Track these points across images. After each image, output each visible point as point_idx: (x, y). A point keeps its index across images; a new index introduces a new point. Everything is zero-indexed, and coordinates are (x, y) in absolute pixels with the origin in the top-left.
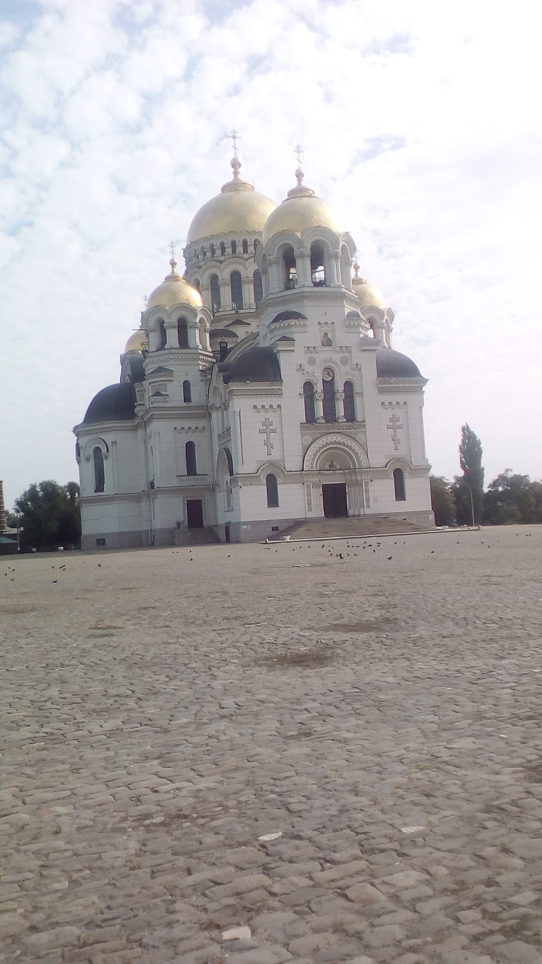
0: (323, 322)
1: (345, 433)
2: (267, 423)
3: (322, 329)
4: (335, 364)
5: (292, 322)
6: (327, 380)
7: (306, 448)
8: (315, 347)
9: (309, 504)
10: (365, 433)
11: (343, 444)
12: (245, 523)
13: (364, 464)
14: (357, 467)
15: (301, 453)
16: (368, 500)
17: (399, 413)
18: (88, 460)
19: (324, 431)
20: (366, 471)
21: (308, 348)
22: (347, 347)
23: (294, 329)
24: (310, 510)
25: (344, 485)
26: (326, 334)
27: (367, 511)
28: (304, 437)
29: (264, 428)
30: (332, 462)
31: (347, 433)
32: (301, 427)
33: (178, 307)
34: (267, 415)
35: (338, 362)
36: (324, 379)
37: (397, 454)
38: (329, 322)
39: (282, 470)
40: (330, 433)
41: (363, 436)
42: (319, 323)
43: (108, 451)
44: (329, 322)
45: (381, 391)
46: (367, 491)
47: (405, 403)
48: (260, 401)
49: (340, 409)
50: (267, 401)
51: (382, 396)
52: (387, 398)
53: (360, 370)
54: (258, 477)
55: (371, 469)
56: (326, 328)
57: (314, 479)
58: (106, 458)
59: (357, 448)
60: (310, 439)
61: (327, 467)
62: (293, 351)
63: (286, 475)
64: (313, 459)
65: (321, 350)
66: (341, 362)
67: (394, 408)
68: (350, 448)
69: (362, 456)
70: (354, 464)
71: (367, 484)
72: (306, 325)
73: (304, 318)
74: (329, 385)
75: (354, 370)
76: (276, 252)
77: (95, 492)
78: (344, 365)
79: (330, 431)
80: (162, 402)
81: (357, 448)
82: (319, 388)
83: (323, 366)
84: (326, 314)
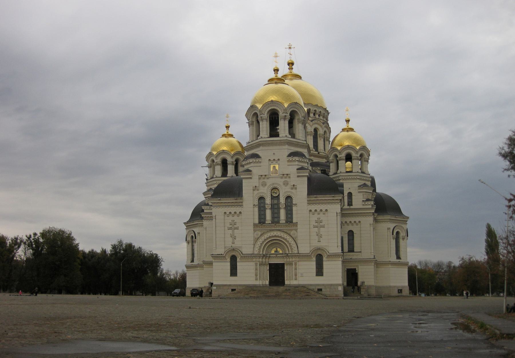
0: (272, 159)
1: (282, 230)
2: (233, 223)
3: (272, 163)
4: (279, 185)
5: (251, 160)
6: (275, 196)
7: (256, 240)
8: (265, 175)
9: (256, 275)
10: (296, 230)
11: (281, 237)
13: (295, 251)
14: (290, 252)
15: (252, 242)
16: (296, 275)
17: (322, 216)
18: (188, 243)
20: (295, 256)
21: (261, 176)
22: (287, 175)
23: (252, 165)
24: (256, 279)
25: (284, 264)
26: (274, 167)
27: (294, 282)
28: (256, 233)
29: (231, 226)
30: (277, 249)
31: (285, 231)
32: (254, 226)
33: (221, 153)
34: (233, 218)
36: (273, 195)
37: (319, 245)
38: (276, 159)
39: (239, 253)
40: (273, 230)
41: (295, 232)
42: (270, 160)
43: (195, 238)
44: (276, 159)
45: (310, 203)
46: (296, 269)
47: (326, 210)
48: (228, 210)
49: (283, 213)
50: (233, 210)
51: (310, 206)
52: (313, 207)
53: (296, 189)
54: (224, 257)
56: (274, 162)
57: (261, 260)
58: (195, 242)
60: (260, 233)
61: (273, 252)
62: (251, 178)
63: (242, 256)
64: (260, 247)
65: (270, 177)
66: (284, 184)
67: (319, 214)
68: (286, 239)
70: (289, 250)
71: (296, 264)
72: (260, 162)
75: (292, 189)
76: (251, 118)
77: (191, 262)
78: (286, 186)
79: (273, 229)
80: (209, 209)
81: (290, 240)
82: (268, 201)
83: (272, 187)
84: (274, 154)
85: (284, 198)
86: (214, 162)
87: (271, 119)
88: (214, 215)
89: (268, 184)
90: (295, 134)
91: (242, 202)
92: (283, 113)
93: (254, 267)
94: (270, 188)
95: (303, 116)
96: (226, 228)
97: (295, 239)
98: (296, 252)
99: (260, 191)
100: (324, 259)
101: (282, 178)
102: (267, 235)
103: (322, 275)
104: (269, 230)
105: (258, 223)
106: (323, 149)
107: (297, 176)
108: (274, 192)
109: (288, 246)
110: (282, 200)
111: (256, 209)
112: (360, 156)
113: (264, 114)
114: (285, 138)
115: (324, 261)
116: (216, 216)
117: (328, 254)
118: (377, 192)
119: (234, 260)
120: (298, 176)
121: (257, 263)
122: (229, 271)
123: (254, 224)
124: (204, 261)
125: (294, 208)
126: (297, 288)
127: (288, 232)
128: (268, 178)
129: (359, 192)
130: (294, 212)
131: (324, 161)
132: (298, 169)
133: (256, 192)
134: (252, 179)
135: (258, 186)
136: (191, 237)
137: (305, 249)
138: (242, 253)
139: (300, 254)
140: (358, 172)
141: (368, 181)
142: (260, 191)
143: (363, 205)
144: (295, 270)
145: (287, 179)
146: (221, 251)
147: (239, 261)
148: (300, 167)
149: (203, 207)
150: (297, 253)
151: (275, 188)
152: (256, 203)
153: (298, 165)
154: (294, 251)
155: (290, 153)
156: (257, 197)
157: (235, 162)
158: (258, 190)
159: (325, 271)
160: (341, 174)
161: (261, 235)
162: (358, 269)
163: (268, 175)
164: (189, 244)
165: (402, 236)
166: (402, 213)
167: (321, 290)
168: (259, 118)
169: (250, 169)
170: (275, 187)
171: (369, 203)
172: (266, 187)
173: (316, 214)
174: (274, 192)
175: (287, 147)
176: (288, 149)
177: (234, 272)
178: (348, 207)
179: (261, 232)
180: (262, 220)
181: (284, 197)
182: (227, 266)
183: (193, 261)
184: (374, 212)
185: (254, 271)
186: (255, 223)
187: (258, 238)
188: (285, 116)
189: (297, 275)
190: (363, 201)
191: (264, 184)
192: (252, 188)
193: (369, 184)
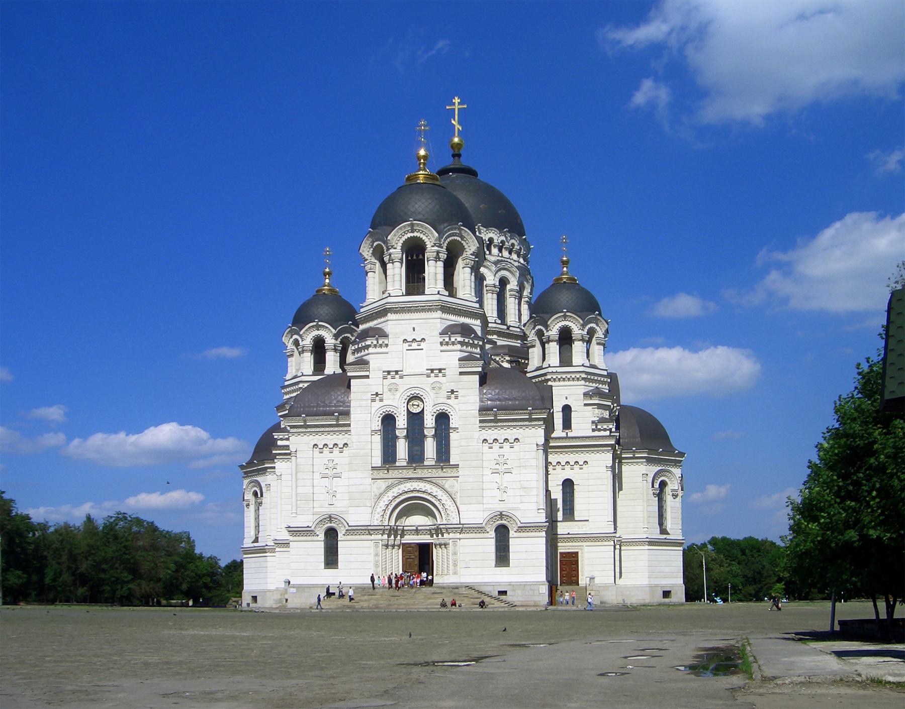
8: (397, 372)
12: (295, 586)
14: (445, 522)
16: (455, 565)
19: (400, 476)
21: (389, 372)
22: (440, 370)
23: (371, 350)
35: (428, 389)
36: (411, 410)
37: (501, 507)
42: (405, 341)
43: (262, 496)
46: (455, 554)
48: (321, 440)
49: (430, 447)
50: (330, 439)
52: (491, 434)
53: (456, 398)
54: (312, 531)
55: (461, 526)
59: (444, 498)
60: (383, 484)
62: (367, 377)
66: (433, 388)
69: (451, 507)
71: (455, 545)
73: (385, 336)
74: (415, 419)
75: (449, 398)
81: (444, 498)
82: (402, 422)
85: (433, 416)
86: (299, 346)
87: (410, 258)
88: (292, 449)
89: (401, 390)
90: (456, 288)
91: (349, 425)
92: (432, 246)
93: (372, 550)
94: (405, 397)
95: (474, 252)
96: (317, 476)
97: (453, 496)
98: (456, 521)
99: (385, 402)
100: (512, 533)
101: (428, 376)
102: (399, 489)
103: (507, 565)
104: (402, 480)
105: (380, 465)
106: (518, 321)
107: (459, 373)
108: (413, 405)
109: (441, 510)
110: (429, 421)
111: (378, 439)
112: (588, 334)
113: (395, 248)
114: (437, 297)
115: (511, 538)
116: (296, 451)
117: (519, 524)
118: (621, 404)
119: (331, 535)
120: (461, 373)
121: (379, 542)
122: (322, 558)
123: (372, 467)
124: (276, 540)
125: (453, 436)
126: (456, 590)
127: (440, 482)
128: (401, 377)
129: (586, 405)
130: (453, 443)
131: (517, 343)
132: (460, 360)
133: (377, 404)
134: (369, 378)
135: (382, 393)
136: (253, 493)
137: (473, 514)
138: (348, 524)
139: (463, 524)
140: (583, 365)
141: (603, 383)
142: (385, 402)
143: (593, 430)
144: (453, 555)
145: (440, 379)
146: (305, 520)
147: (342, 539)
148: (466, 354)
149: (276, 435)
150: (459, 523)
151: (416, 397)
152: (377, 425)
153: (461, 351)
154: (451, 519)
155: (446, 325)
156: (379, 415)
157: (341, 346)
158: (381, 400)
159: (512, 556)
160: (550, 370)
161: (389, 488)
162: (582, 553)
163: (402, 371)
164: (248, 508)
165: (673, 490)
166: (673, 447)
167: (504, 593)
168: (386, 259)
169: (365, 358)
170: (415, 395)
171: (605, 427)
172: (398, 394)
173: (496, 446)
174: (413, 405)
175: (439, 314)
176: (441, 318)
177: (331, 558)
178: (564, 435)
179: (387, 483)
180: (389, 456)
181: (433, 414)
182: (318, 547)
183: (256, 540)
184: (614, 443)
185: (372, 558)
186: (373, 465)
187: (381, 495)
188: (438, 252)
189: (457, 565)
190: (593, 422)
191: (393, 389)
192: (370, 397)
193: (605, 388)
